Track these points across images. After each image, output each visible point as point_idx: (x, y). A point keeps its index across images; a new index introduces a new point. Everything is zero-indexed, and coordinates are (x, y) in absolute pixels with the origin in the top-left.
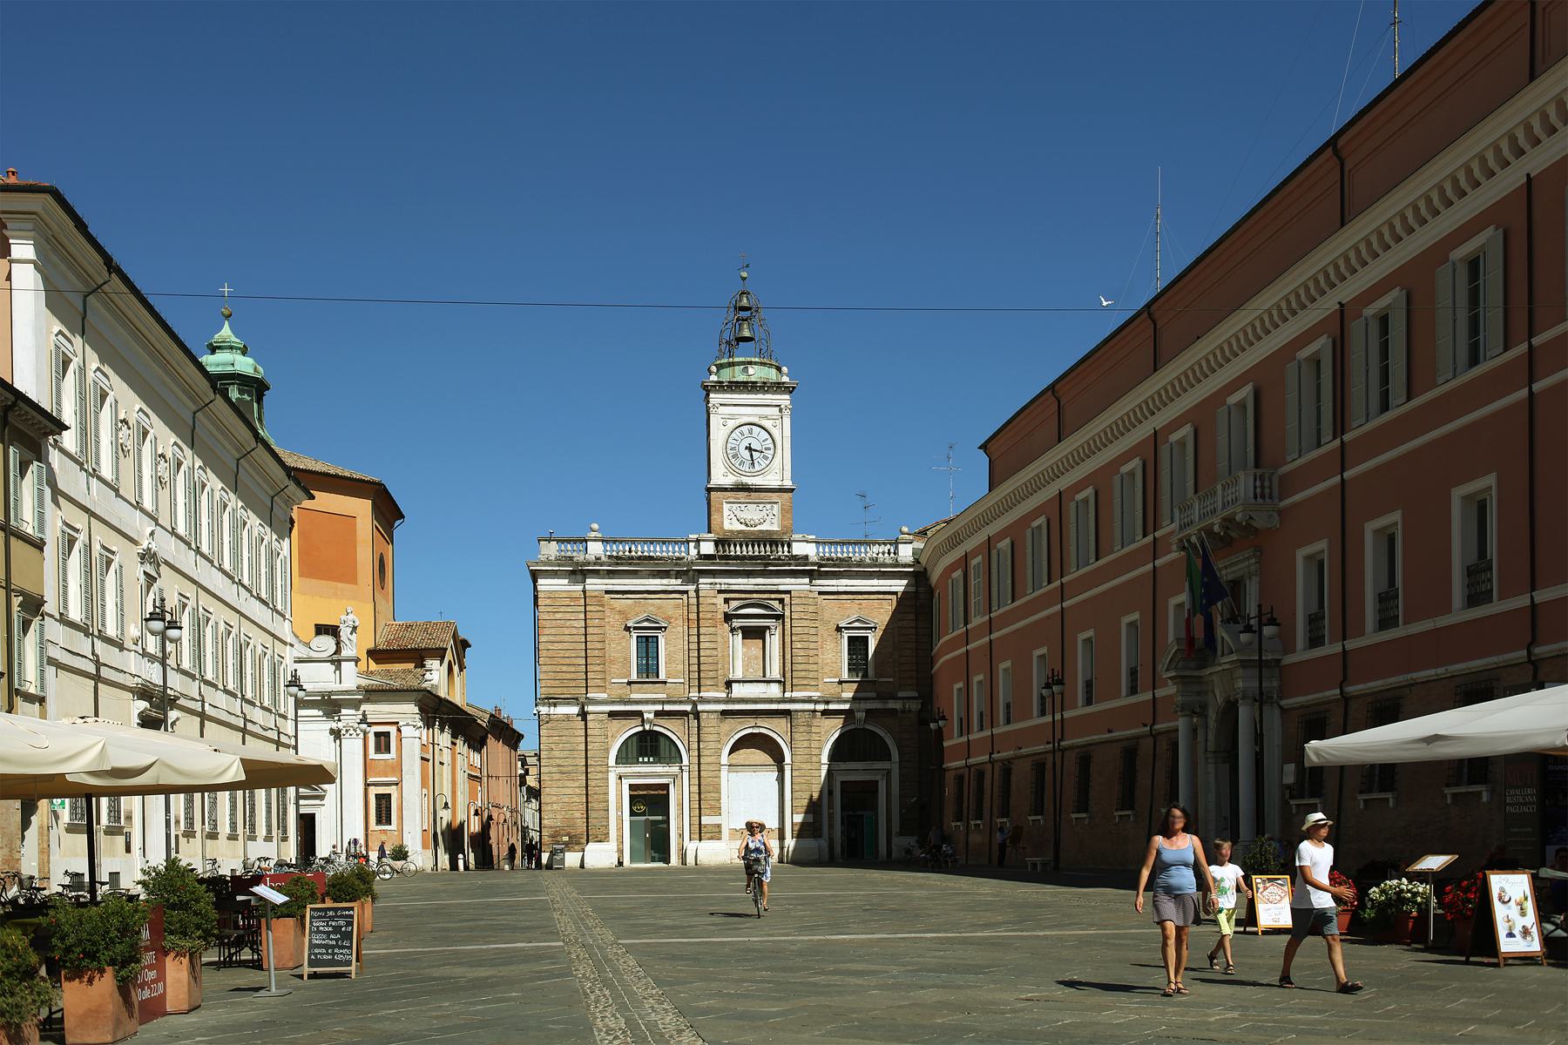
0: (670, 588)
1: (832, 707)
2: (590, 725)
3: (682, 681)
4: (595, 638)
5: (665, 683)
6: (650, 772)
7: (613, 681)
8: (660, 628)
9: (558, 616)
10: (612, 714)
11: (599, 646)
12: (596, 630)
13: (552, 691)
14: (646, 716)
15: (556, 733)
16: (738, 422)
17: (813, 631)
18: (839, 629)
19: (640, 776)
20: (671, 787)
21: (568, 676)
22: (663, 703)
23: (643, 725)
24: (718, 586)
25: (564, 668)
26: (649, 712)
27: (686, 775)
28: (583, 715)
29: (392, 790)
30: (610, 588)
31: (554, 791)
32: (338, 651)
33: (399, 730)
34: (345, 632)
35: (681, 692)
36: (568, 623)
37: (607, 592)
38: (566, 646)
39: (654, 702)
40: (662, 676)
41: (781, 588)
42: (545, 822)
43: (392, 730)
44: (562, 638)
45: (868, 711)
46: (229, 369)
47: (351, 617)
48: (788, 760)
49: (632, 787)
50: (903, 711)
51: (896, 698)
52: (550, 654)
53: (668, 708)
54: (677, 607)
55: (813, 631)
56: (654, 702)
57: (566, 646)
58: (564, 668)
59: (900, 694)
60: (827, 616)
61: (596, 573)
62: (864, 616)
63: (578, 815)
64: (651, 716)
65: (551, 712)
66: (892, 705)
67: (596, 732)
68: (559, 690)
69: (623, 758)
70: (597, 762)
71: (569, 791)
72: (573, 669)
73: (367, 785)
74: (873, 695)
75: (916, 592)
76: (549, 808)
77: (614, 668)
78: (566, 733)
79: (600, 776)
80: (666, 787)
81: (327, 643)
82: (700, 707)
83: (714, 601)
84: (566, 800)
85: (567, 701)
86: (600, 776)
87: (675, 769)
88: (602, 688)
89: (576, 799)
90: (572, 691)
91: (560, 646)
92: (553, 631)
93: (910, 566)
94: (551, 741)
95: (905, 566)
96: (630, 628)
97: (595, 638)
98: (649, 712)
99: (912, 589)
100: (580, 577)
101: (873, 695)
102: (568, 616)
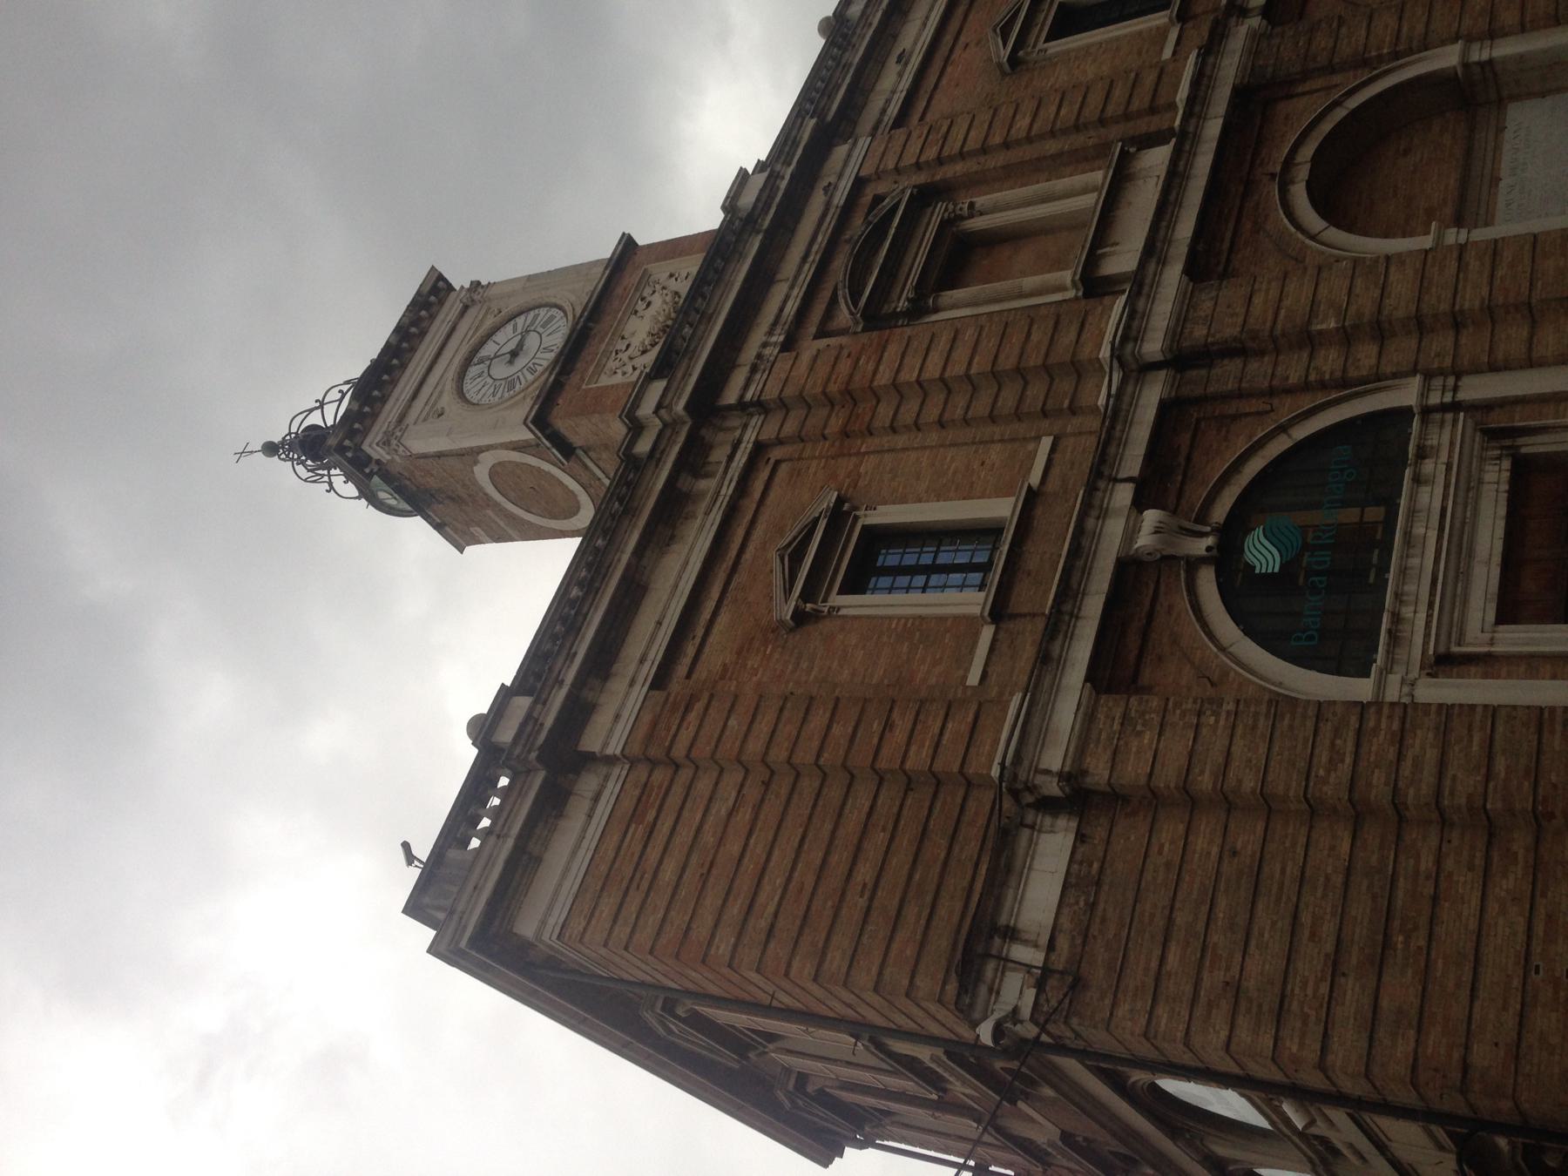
2: (1133, 770)
3: (1047, 442)
5: (1032, 497)
7: (974, 678)
9: (668, 873)
13: (941, 942)
16: (449, 385)
20: (1534, 446)
21: (900, 861)
23: (1193, 564)
24: (767, 351)
25: (865, 873)
26: (1131, 534)
27: (1476, 389)
30: (649, 670)
36: (709, 838)
41: (840, 198)
44: (749, 866)
48: (1447, 58)
49: (1509, 610)
53: (1132, 460)
58: (865, 873)
62: (1003, 12)
65: (1035, 957)
67: (1176, 748)
68: (950, 909)
70: (1332, 764)
72: (879, 838)
79: (1423, 744)
82: (1153, 346)
83: (806, 357)
86: (1423, 744)
88: (984, 706)
90: (969, 847)
91: (774, 881)
92: (711, 901)
96: (800, 618)
98: (1131, 534)
102: (684, 836)
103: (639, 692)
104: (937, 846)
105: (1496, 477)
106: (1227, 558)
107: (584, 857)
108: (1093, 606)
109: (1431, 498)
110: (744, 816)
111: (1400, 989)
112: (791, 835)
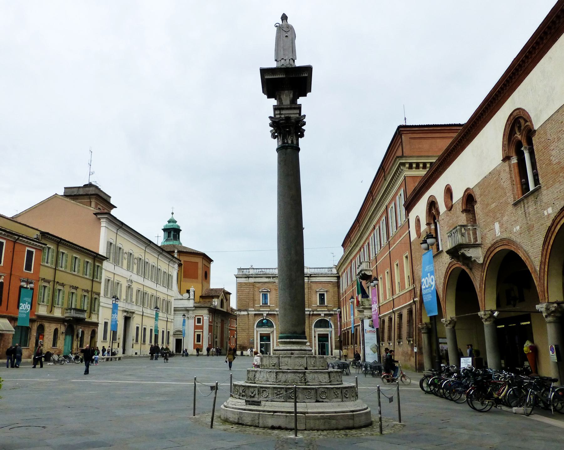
0: (271, 281)
1: (314, 313)
4: (251, 294)
5: (270, 306)
6: (265, 330)
8: (268, 292)
9: (242, 288)
10: (255, 315)
11: (252, 296)
12: (251, 292)
14: (264, 315)
15: (241, 319)
17: (309, 292)
18: (317, 292)
19: (263, 331)
20: (271, 334)
21: (244, 304)
22: (269, 311)
25: (243, 302)
28: (248, 314)
29: (201, 334)
30: (255, 281)
31: (240, 335)
32: (189, 297)
33: (203, 318)
34: (192, 293)
35: (273, 309)
37: (254, 282)
38: (243, 296)
39: (267, 311)
40: (269, 304)
42: (238, 343)
43: (201, 317)
44: (243, 294)
45: (325, 314)
46: (172, 227)
47: (193, 288)
50: (335, 314)
51: (333, 311)
52: (240, 298)
53: (270, 313)
54: (273, 286)
55: (309, 292)
56: (267, 311)
57: (243, 296)
58: (243, 302)
59: (334, 309)
60: (313, 288)
61: (252, 277)
63: (246, 341)
64: (266, 315)
66: (331, 312)
68: (242, 308)
69: (258, 326)
71: (244, 335)
72: (245, 302)
73: (195, 332)
74: (327, 309)
75: (338, 281)
76: (239, 339)
77: (256, 302)
78: (244, 319)
79: (252, 331)
80: (270, 334)
81: (186, 295)
84: (243, 337)
85: (244, 311)
86: (252, 331)
87: (271, 329)
89: (246, 337)
92: (241, 292)
93: (336, 274)
94: (239, 321)
95: (334, 274)
97: (251, 294)
99: (337, 281)
100: (247, 279)
101: (327, 309)
102: (244, 289)
103: (254, 281)
104: (246, 306)
105: (269, 333)
106: (264, 319)
107: (242, 281)
108: (260, 313)
109: (268, 329)
110: (246, 292)
111: (241, 331)
112: (245, 296)
